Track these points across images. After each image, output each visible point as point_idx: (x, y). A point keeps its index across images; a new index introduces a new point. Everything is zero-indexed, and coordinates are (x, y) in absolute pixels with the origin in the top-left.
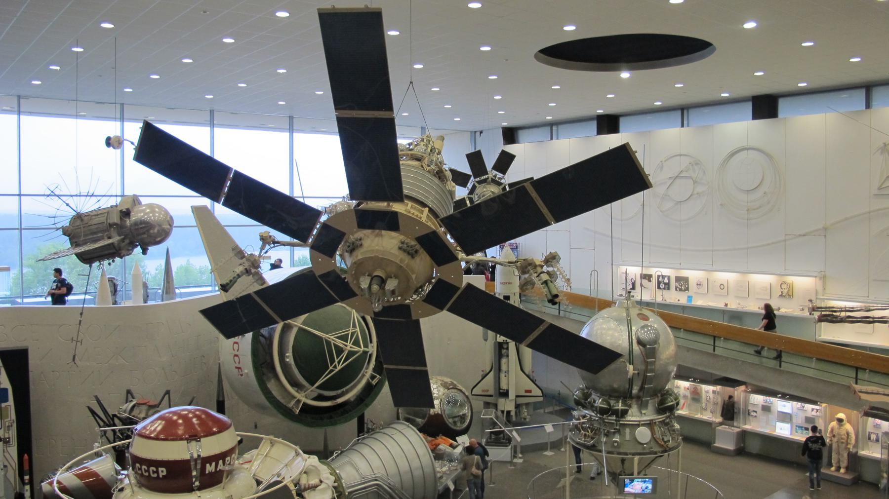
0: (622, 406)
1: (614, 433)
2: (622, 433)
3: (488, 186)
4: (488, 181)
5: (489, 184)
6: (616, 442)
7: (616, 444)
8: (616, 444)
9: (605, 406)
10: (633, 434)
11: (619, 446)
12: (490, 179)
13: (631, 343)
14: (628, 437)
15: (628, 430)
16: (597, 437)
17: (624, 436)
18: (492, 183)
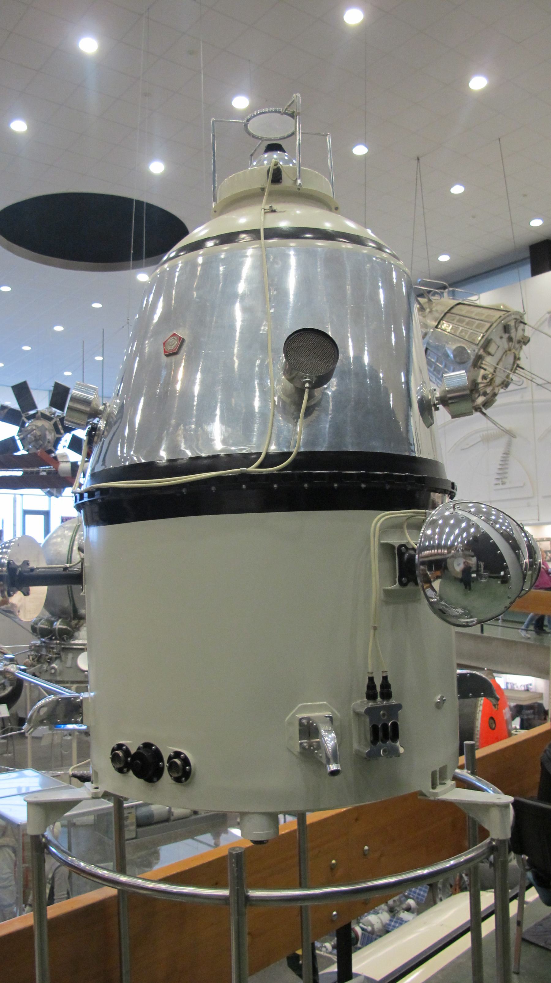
0: (60, 625)
1: (56, 658)
2: (63, 657)
3: (37, 421)
4: (37, 415)
5: (38, 419)
6: (53, 668)
7: (53, 671)
8: (53, 671)
9: (45, 627)
10: (75, 659)
11: (54, 674)
12: (39, 414)
13: (70, 550)
14: (69, 664)
15: (70, 656)
16: (39, 665)
17: (66, 662)
18: (41, 418)
